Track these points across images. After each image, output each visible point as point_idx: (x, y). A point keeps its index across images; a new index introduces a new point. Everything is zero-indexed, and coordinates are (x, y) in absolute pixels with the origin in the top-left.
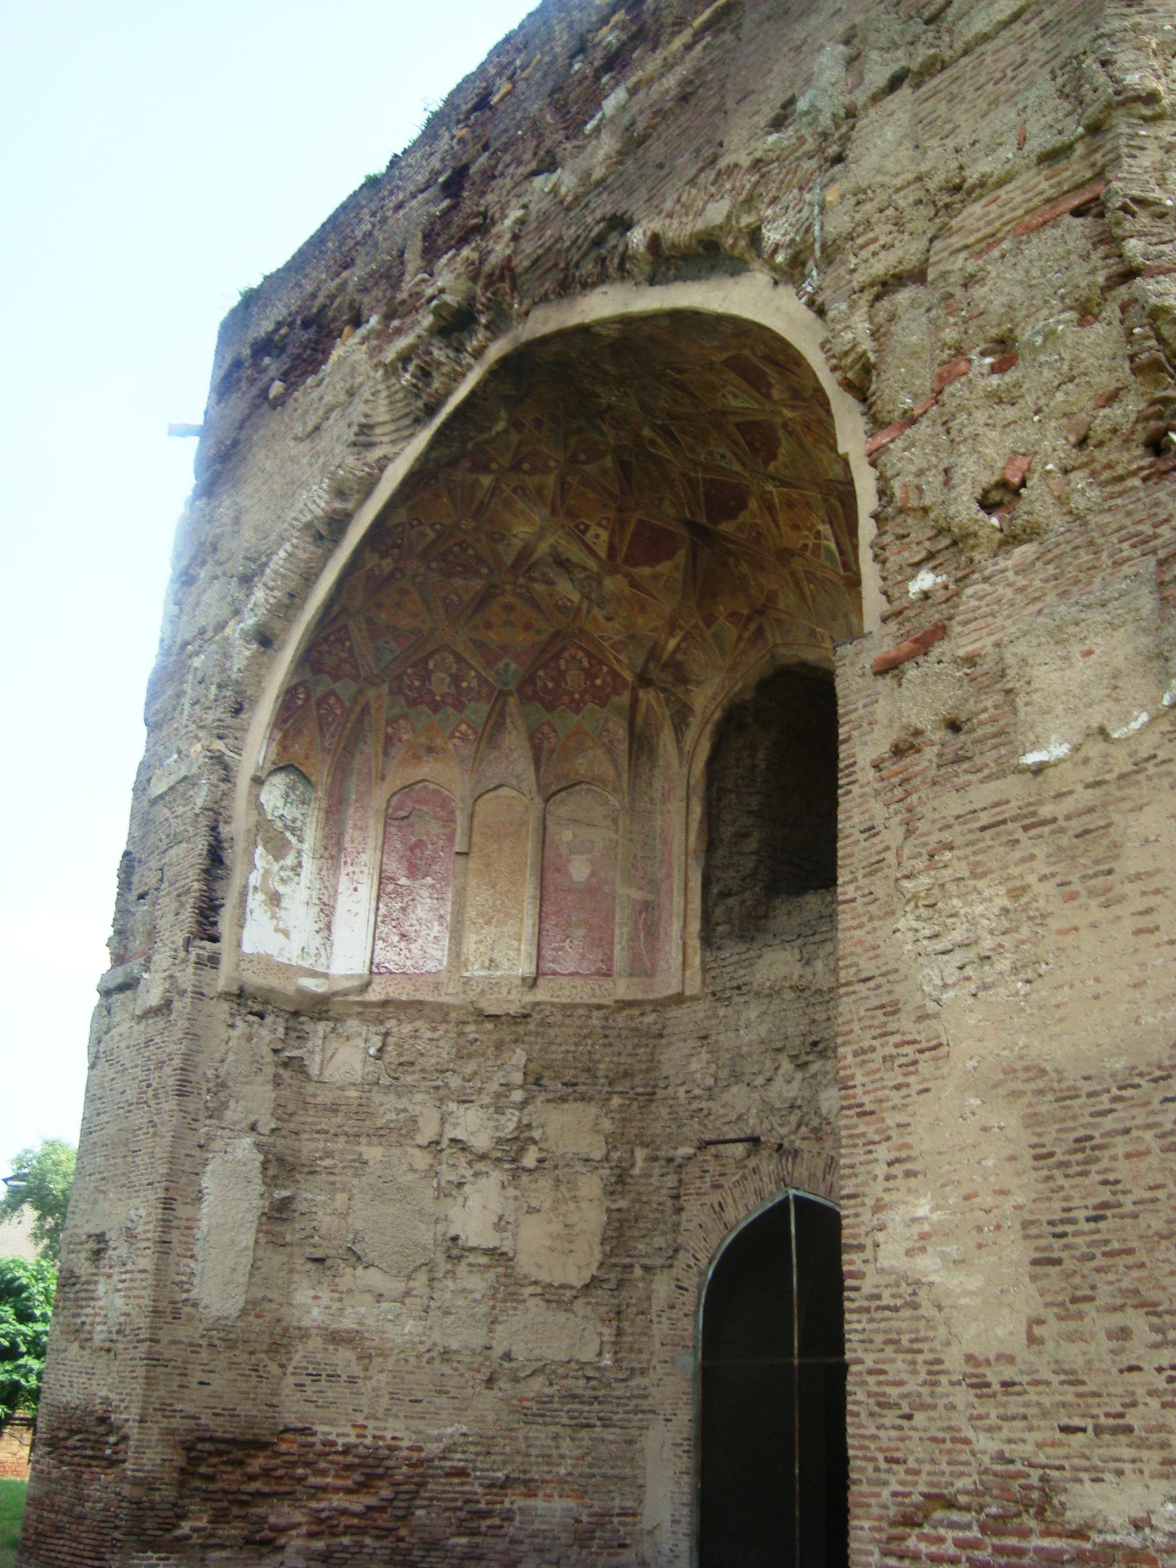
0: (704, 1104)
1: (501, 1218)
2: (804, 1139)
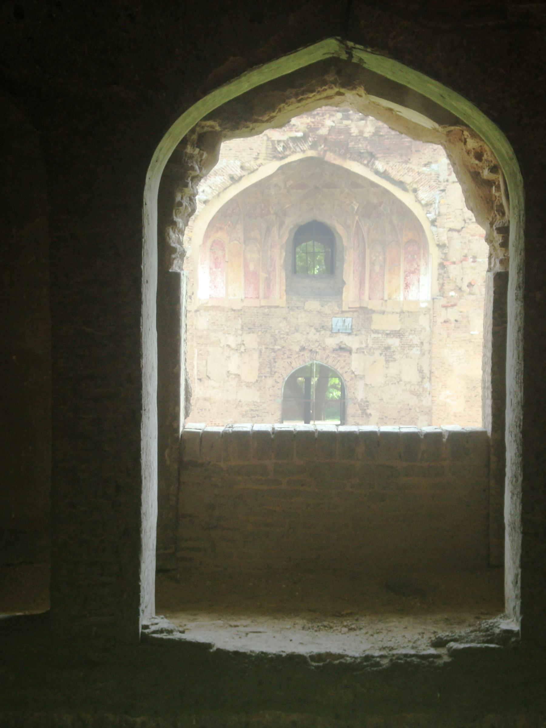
0: (284, 336)
1: (238, 365)
2: (320, 349)
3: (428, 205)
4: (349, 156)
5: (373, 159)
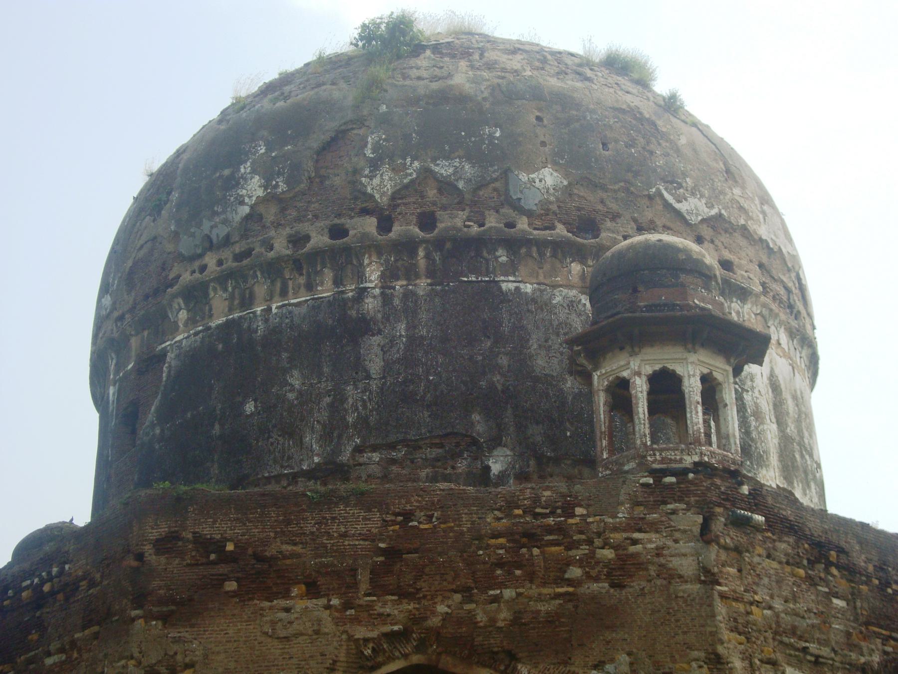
4: (476, 660)
5: (513, 663)
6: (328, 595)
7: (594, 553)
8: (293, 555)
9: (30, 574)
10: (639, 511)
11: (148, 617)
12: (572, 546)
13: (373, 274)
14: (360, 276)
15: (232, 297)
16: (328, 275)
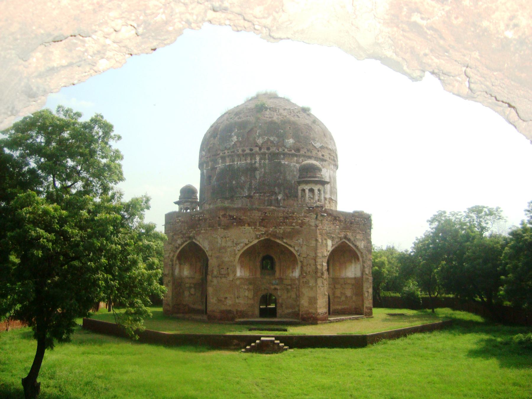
3: (297, 251)
6: (251, 226)
7: (297, 221)
8: (246, 219)
9: (197, 214)
10: (306, 214)
11: (221, 228)
12: (294, 220)
13: (258, 159)
14: (255, 159)
15: (230, 160)
16: (249, 158)
